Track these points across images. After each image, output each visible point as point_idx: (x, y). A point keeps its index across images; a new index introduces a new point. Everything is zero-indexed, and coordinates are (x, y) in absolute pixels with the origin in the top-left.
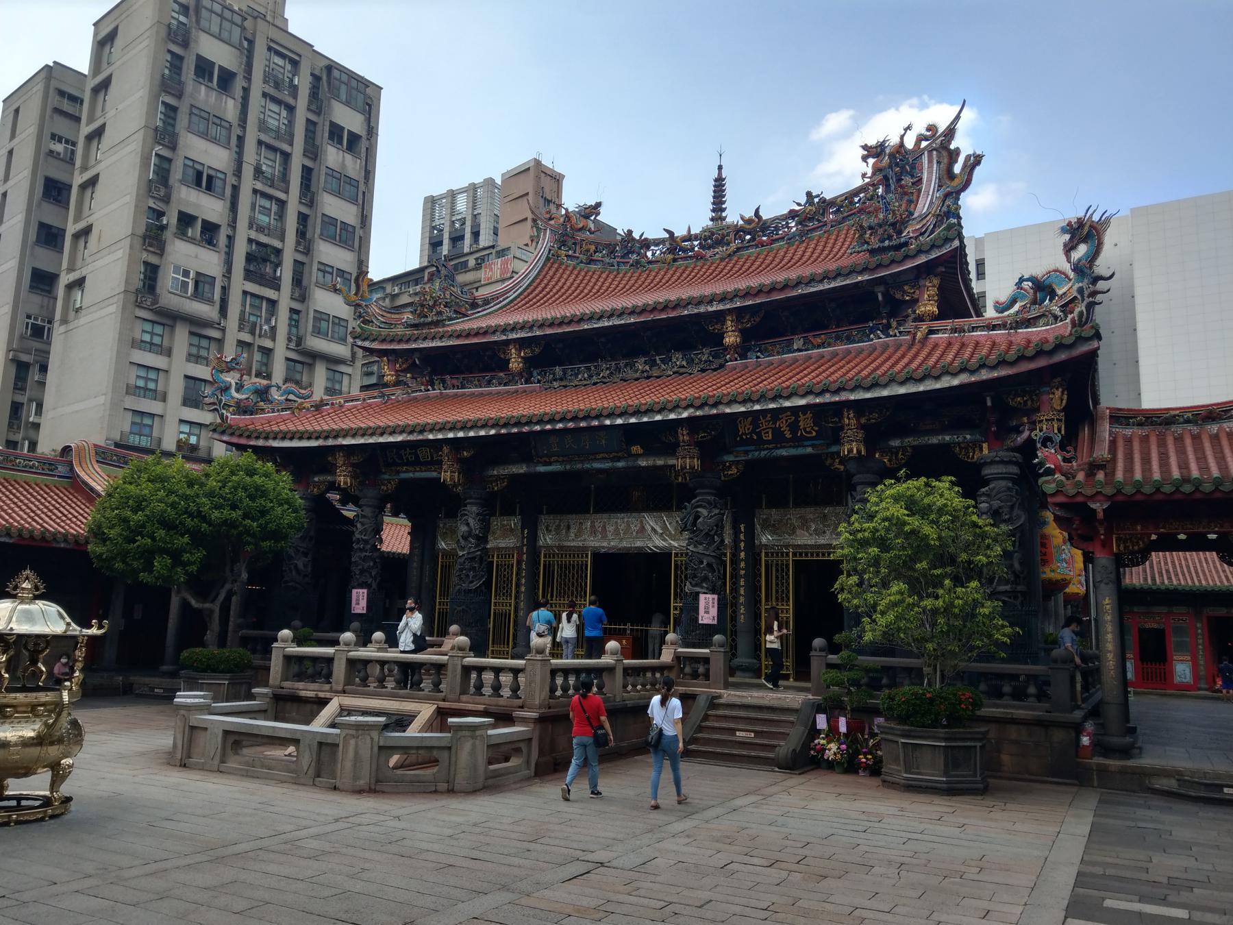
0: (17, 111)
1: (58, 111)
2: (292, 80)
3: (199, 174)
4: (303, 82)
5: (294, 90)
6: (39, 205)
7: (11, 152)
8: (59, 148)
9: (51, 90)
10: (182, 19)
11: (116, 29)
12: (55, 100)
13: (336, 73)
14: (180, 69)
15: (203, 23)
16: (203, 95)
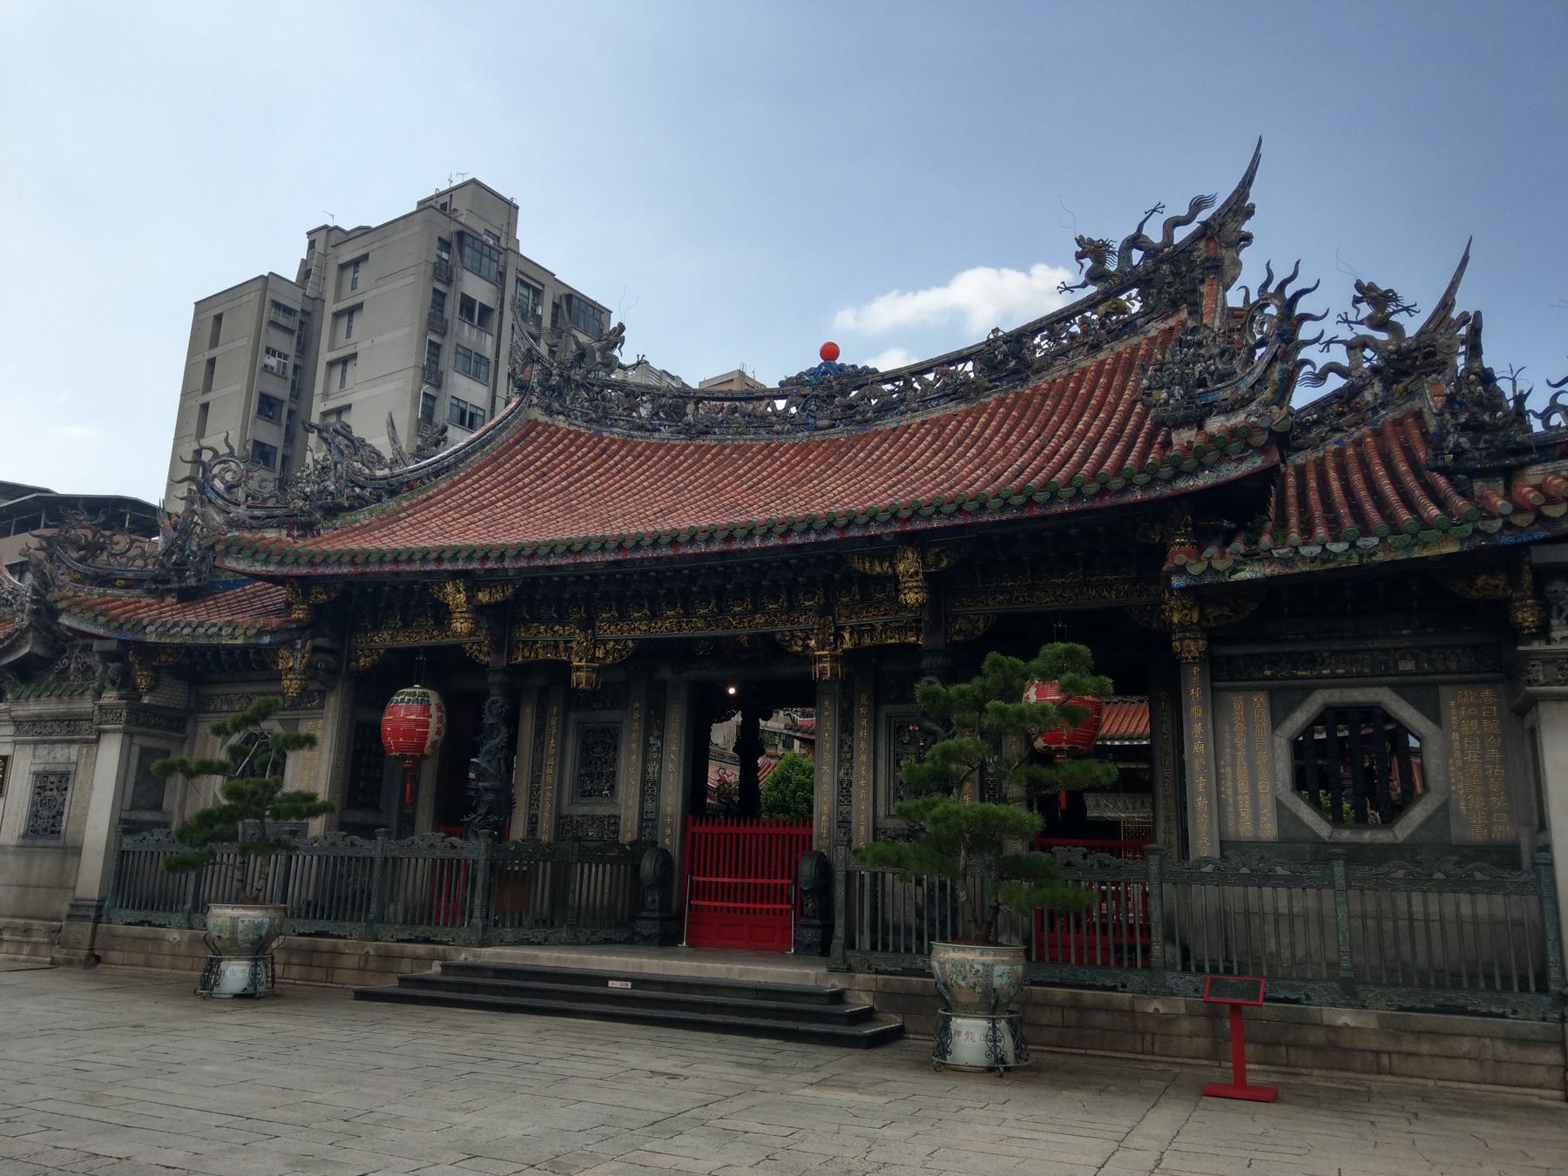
0: (218, 318)
1: (274, 324)
2: (534, 310)
3: (463, 412)
4: (545, 311)
5: (538, 319)
6: (254, 423)
7: (212, 363)
8: (273, 361)
9: (268, 304)
10: (445, 255)
11: (365, 257)
12: (270, 312)
13: (575, 302)
14: (442, 306)
15: (468, 262)
16: (467, 334)
